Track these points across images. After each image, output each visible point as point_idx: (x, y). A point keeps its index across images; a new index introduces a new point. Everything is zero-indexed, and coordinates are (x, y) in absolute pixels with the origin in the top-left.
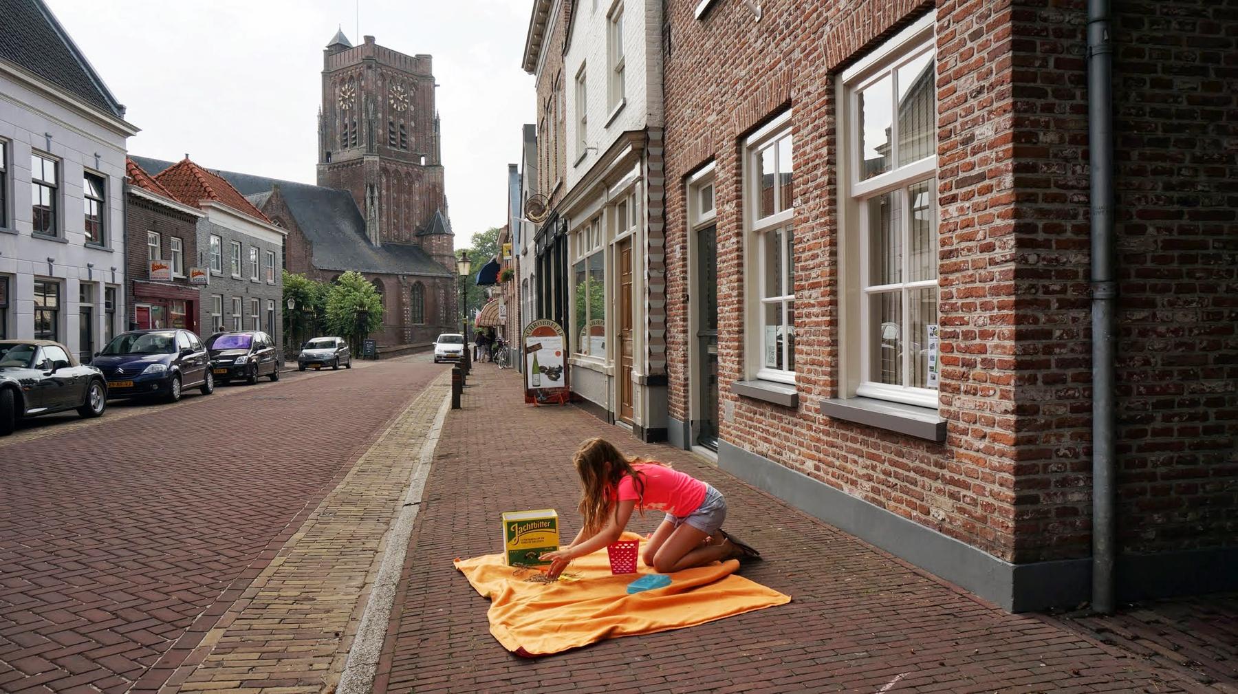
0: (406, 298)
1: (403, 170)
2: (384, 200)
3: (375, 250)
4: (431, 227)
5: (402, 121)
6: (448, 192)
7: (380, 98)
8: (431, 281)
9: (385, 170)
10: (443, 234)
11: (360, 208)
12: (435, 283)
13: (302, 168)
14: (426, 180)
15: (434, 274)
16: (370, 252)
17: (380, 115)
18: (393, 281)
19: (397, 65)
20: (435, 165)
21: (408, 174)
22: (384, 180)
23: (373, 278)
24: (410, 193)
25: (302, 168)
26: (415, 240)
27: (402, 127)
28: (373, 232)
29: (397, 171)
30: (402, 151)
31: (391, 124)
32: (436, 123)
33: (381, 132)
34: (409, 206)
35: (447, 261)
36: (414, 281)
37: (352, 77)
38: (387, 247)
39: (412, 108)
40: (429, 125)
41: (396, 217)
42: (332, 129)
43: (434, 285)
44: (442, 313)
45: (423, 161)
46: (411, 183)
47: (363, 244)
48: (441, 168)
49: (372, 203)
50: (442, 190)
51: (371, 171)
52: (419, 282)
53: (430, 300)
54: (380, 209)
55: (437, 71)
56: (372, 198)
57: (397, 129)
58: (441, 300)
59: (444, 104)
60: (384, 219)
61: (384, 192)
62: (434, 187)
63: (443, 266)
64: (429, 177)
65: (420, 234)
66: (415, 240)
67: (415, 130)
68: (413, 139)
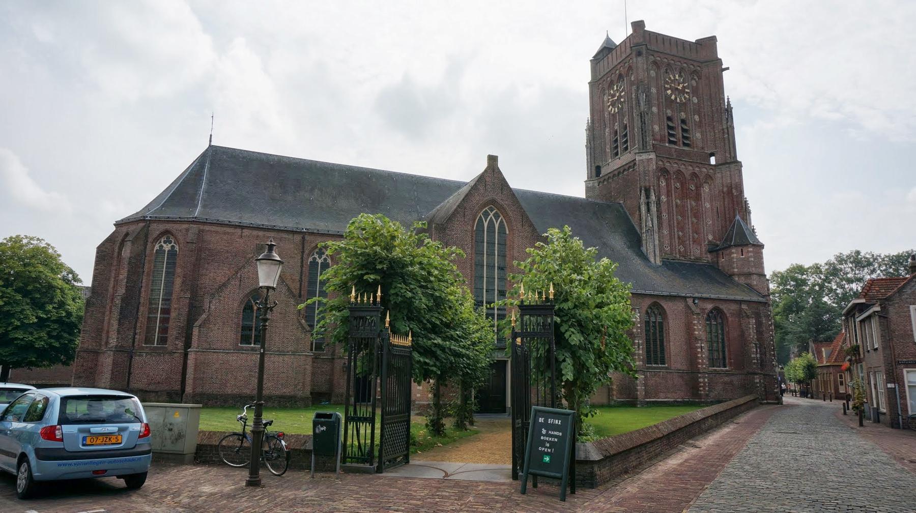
0: (699, 330)
1: (687, 170)
2: (664, 207)
3: (655, 269)
4: (729, 239)
5: (683, 115)
6: (750, 192)
7: (654, 90)
8: (734, 307)
9: (664, 172)
10: (747, 244)
11: (634, 221)
12: (741, 310)
13: (573, 184)
14: (718, 181)
15: (739, 298)
16: (647, 271)
17: (655, 109)
18: (680, 306)
19: (674, 52)
20: (732, 163)
21: (694, 174)
22: (663, 184)
23: (648, 302)
24: (698, 197)
25: (573, 184)
26: (708, 258)
27: (683, 121)
28: (651, 246)
29: (679, 172)
30: (686, 148)
31: (669, 119)
32: (729, 110)
33: (656, 128)
34: (697, 215)
35: (755, 281)
36: (709, 306)
37: (620, 76)
38: (670, 265)
39: (695, 100)
40: (720, 118)
41: (682, 229)
42: (604, 138)
43: (740, 314)
44: (754, 354)
45: (713, 160)
46: (698, 187)
47: (637, 261)
48: (739, 165)
49: (649, 210)
50: (741, 192)
51: (646, 173)
52: (717, 310)
53: (734, 334)
54: (659, 217)
56: (648, 204)
57: (677, 123)
58: (752, 334)
59: (734, 87)
60: (666, 232)
61: (664, 198)
62: (730, 192)
63: (750, 287)
64: (722, 179)
65: (714, 250)
66: (708, 258)
67: (700, 125)
68: (698, 135)
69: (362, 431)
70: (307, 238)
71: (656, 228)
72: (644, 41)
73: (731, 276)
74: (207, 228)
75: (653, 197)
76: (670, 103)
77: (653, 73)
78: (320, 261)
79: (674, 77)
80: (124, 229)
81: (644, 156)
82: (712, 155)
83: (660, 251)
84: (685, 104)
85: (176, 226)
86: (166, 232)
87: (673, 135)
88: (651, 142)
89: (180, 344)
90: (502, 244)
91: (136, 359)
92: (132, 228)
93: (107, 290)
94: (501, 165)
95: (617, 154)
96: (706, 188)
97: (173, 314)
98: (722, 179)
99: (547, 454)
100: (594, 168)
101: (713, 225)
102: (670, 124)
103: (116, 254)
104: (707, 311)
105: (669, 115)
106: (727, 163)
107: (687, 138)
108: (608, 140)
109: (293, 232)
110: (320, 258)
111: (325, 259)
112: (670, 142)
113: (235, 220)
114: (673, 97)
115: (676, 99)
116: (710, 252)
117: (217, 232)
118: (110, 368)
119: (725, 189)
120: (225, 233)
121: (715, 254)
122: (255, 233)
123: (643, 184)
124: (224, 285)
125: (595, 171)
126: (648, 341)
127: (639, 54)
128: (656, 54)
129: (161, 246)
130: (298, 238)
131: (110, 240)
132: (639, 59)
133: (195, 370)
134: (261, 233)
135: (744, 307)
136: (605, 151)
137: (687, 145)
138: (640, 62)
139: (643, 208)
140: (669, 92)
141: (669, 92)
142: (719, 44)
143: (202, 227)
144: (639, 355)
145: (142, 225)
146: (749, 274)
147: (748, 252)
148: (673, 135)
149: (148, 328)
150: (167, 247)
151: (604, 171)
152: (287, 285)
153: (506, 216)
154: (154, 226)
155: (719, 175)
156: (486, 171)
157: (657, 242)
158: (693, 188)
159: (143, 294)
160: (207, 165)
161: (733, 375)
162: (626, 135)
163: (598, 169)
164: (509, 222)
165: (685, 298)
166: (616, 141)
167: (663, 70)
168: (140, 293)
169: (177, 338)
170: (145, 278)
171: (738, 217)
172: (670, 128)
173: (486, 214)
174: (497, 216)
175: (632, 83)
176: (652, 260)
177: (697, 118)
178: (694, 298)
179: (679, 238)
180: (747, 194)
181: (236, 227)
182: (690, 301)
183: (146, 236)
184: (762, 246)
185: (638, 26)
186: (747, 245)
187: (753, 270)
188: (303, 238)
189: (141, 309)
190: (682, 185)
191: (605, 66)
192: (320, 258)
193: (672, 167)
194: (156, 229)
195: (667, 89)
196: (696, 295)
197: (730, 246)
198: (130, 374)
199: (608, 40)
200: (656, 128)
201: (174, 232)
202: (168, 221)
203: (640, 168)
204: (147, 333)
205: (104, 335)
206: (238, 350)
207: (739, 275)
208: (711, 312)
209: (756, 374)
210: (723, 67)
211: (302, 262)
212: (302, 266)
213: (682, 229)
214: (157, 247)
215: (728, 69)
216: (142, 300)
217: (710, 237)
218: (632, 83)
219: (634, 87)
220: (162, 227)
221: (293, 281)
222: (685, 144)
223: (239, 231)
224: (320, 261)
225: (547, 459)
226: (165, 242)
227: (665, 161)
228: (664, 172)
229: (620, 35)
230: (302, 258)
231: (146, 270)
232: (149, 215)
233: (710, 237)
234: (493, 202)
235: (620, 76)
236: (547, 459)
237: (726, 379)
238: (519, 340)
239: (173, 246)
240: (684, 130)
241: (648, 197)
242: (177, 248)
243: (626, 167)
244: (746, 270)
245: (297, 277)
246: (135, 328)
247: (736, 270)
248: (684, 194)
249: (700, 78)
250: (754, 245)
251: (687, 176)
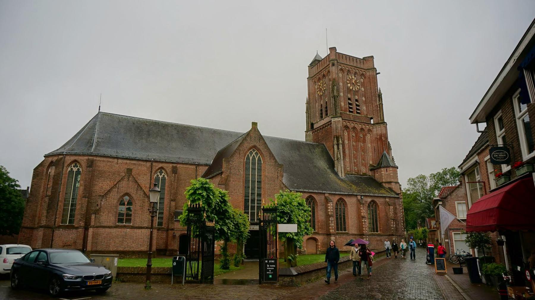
0: (364, 212)
1: (359, 127)
2: (346, 147)
5: (357, 97)
7: (341, 84)
8: (382, 200)
11: (331, 153)
12: (386, 202)
13: (299, 133)
21: (362, 129)
24: (364, 141)
26: (370, 173)
27: (357, 100)
28: (340, 167)
29: (354, 128)
31: (349, 99)
34: (364, 150)
35: (393, 186)
36: (369, 200)
39: (363, 89)
41: (356, 158)
46: (364, 136)
47: (332, 176)
49: (338, 148)
50: (387, 138)
52: (373, 201)
54: (344, 152)
55: (377, 64)
59: (383, 84)
60: (347, 160)
62: (381, 138)
63: (390, 189)
67: (365, 102)
68: (365, 108)
69: (193, 265)
70: (154, 164)
71: (342, 158)
72: (336, 58)
74: (98, 159)
75: (341, 142)
76: (349, 91)
77: (340, 75)
78: (161, 177)
80: (50, 159)
81: (336, 119)
82: (372, 118)
83: (344, 169)
84: (357, 91)
85: (81, 158)
86: (75, 161)
87: (351, 108)
88: (339, 111)
89: (82, 224)
90: (260, 170)
91: (57, 232)
92: (55, 159)
93: (39, 193)
94: (259, 127)
95: (322, 117)
96: (368, 137)
97: (78, 207)
98: (377, 130)
99: (270, 274)
100: (310, 125)
101: (372, 156)
102: (349, 101)
103: (45, 173)
104: (368, 202)
106: (379, 123)
107: (358, 109)
108: (317, 110)
109: (146, 161)
110: (161, 175)
111: (164, 176)
112: (350, 112)
113: (114, 154)
114: (351, 88)
116: (371, 170)
117: (103, 161)
118: (42, 237)
119: (378, 137)
120: (108, 161)
121: (373, 172)
122: (125, 161)
123: (335, 134)
124: (109, 191)
125: (311, 126)
126: (337, 219)
127: (333, 65)
128: (342, 65)
129: (72, 169)
130: (149, 164)
131: (41, 165)
132: (334, 67)
133: (93, 237)
134: (128, 162)
135: (387, 200)
136: (316, 116)
138: (333, 69)
139: (336, 147)
140: (349, 85)
141: (349, 85)
143: (95, 158)
144: (332, 226)
145: (60, 157)
146: (390, 183)
147: (390, 171)
148: (351, 108)
149: (63, 214)
150: (75, 169)
151: (315, 126)
152: (143, 191)
153: (261, 154)
154: (67, 158)
155: (375, 130)
156: (251, 130)
157: (342, 165)
159: (61, 196)
160: (98, 124)
161: (382, 236)
162: (326, 108)
163: (312, 125)
164: (263, 156)
165: (357, 195)
166: (322, 110)
167: (346, 73)
168: (59, 195)
169: (80, 220)
170: (62, 186)
171: (385, 152)
172: (350, 104)
173: (251, 153)
174: (256, 154)
175: (330, 80)
176: (340, 175)
177: (364, 99)
178: (361, 196)
179: (354, 163)
180: (389, 140)
181: (114, 158)
182: (359, 197)
183: (63, 164)
185: (333, 49)
186: (389, 167)
187: (393, 180)
188: (152, 164)
189: (60, 204)
191: (315, 70)
192: (161, 175)
193: (351, 125)
194: (69, 159)
195: (347, 83)
196: (362, 194)
197: (381, 167)
198: (52, 240)
199: (317, 55)
200: (343, 104)
201: (80, 161)
202: (75, 155)
203: (333, 126)
204: (63, 217)
205: (37, 219)
206: (117, 227)
207: (385, 183)
208: (370, 203)
209: (393, 235)
211: (151, 178)
212: (151, 180)
213: (356, 158)
214: (69, 169)
216: (60, 199)
217: (371, 163)
218: (330, 80)
219: (331, 82)
220: (73, 158)
221: (146, 187)
222: (357, 113)
223: (116, 160)
224: (161, 177)
225: (271, 276)
226: (74, 166)
227: (347, 121)
228: (346, 127)
229: (324, 54)
230: (151, 175)
231: (63, 182)
232: (65, 151)
234: (255, 147)
235: (324, 76)
236: (271, 276)
237: (378, 238)
238: (262, 223)
239: (78, 169)
240: (357, 105)
241: (338, 141)
242: (81, 170)
243: (327, 125)
244: (389, 180)
245: (148, 186)
246: (56, 215)
248: (357, 140)
249: (365, 78)
250: (392, 167)
251: (359, 131)
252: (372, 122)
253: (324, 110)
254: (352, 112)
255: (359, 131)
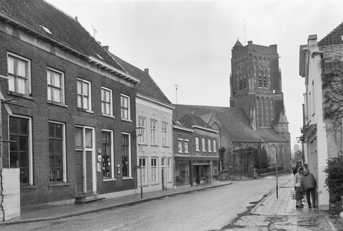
1: (265, 96)
21: (268, 98)
27: (264, 77)
29: (263, 97)
30: (265, 88)
55: (279, 51)
73: (278, 133)
79: (262, 61)
82: (274, 89)
87: (261, 84)
105: (260, 76)
107: (266, 84)
114: (261, 69)
115: (262, 70)
137: (266, 87)
142: (278, 47)
148: (261, 84)
158: (267, 102)
184: (288, 123)
190: (263, 102)
199: (238, 42)
210: (279, 56)
215: (280, 57)
222: (265, 86)
227: (258, 94)
233: (272, 119)
247: (280, 131)
251: (265, 98)
252: (274, 92)
253: (243, 84)
254: (261, 86)
255: (265, 98)
